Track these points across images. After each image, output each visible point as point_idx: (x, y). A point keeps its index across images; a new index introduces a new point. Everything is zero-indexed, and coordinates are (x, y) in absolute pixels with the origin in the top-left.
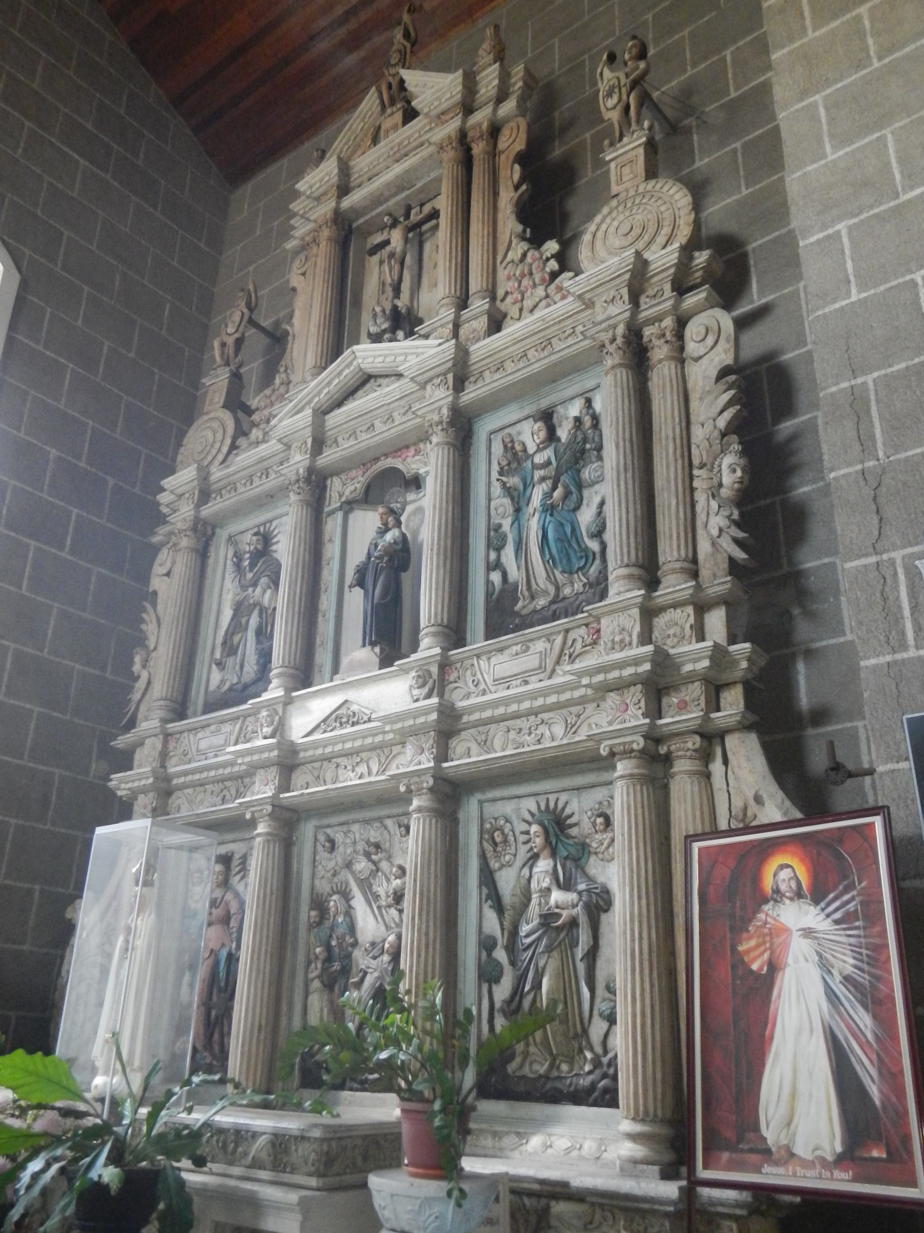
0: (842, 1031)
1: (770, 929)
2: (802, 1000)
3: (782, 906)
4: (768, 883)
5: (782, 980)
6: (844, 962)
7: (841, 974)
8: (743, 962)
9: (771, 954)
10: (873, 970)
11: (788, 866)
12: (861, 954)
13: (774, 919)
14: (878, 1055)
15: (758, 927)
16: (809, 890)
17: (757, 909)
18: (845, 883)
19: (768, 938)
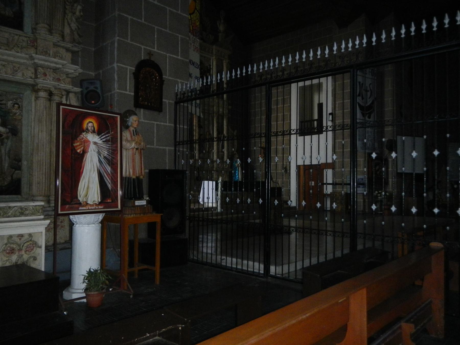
0: (102, 171)
1: (84, 140)
2: (92, 162)
3: (88, 134)
4: (85, 126)
5: (87, 155)
6: (105, 153)
7: (103, 156)
8: (74, 148)
9: (84, 148)
10: (113, 156)
11: (92, 122)
12: (109, 151)
13: (86, 137)
14: (111, 177)
15: (80, 139)
16: (97, 131)
17: (81, 134)
18: (107, 131)
19: (83, 143)
